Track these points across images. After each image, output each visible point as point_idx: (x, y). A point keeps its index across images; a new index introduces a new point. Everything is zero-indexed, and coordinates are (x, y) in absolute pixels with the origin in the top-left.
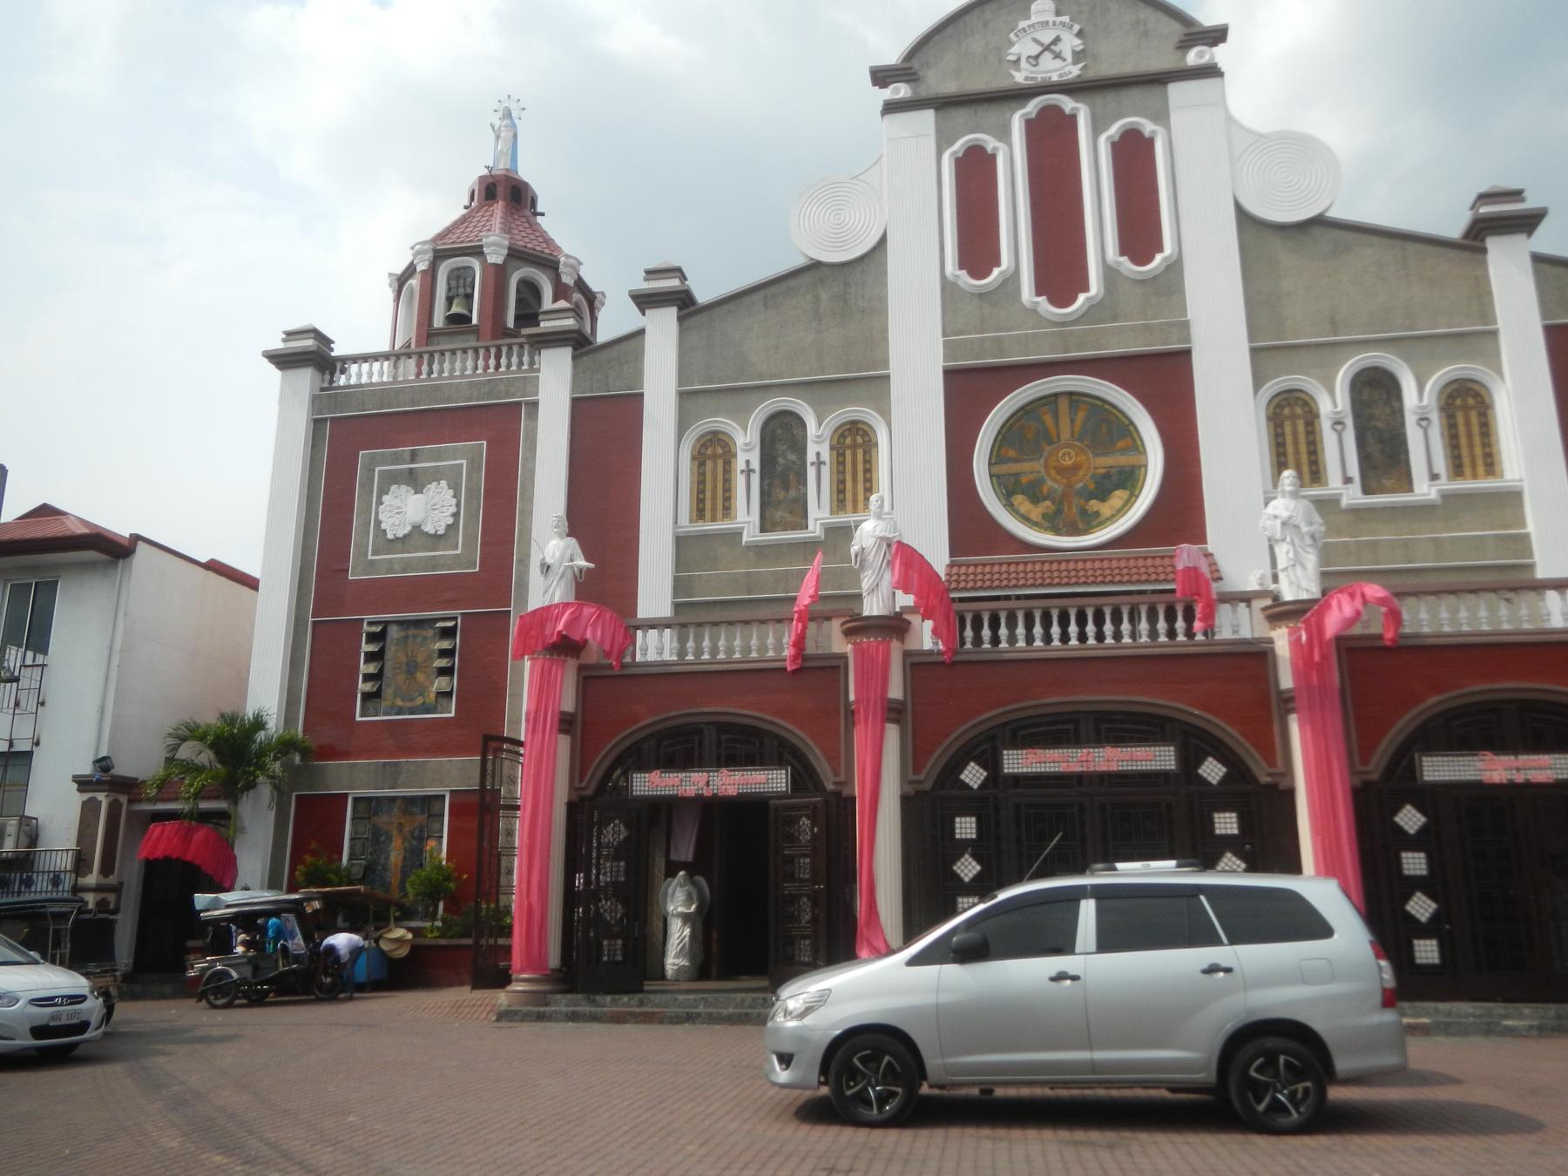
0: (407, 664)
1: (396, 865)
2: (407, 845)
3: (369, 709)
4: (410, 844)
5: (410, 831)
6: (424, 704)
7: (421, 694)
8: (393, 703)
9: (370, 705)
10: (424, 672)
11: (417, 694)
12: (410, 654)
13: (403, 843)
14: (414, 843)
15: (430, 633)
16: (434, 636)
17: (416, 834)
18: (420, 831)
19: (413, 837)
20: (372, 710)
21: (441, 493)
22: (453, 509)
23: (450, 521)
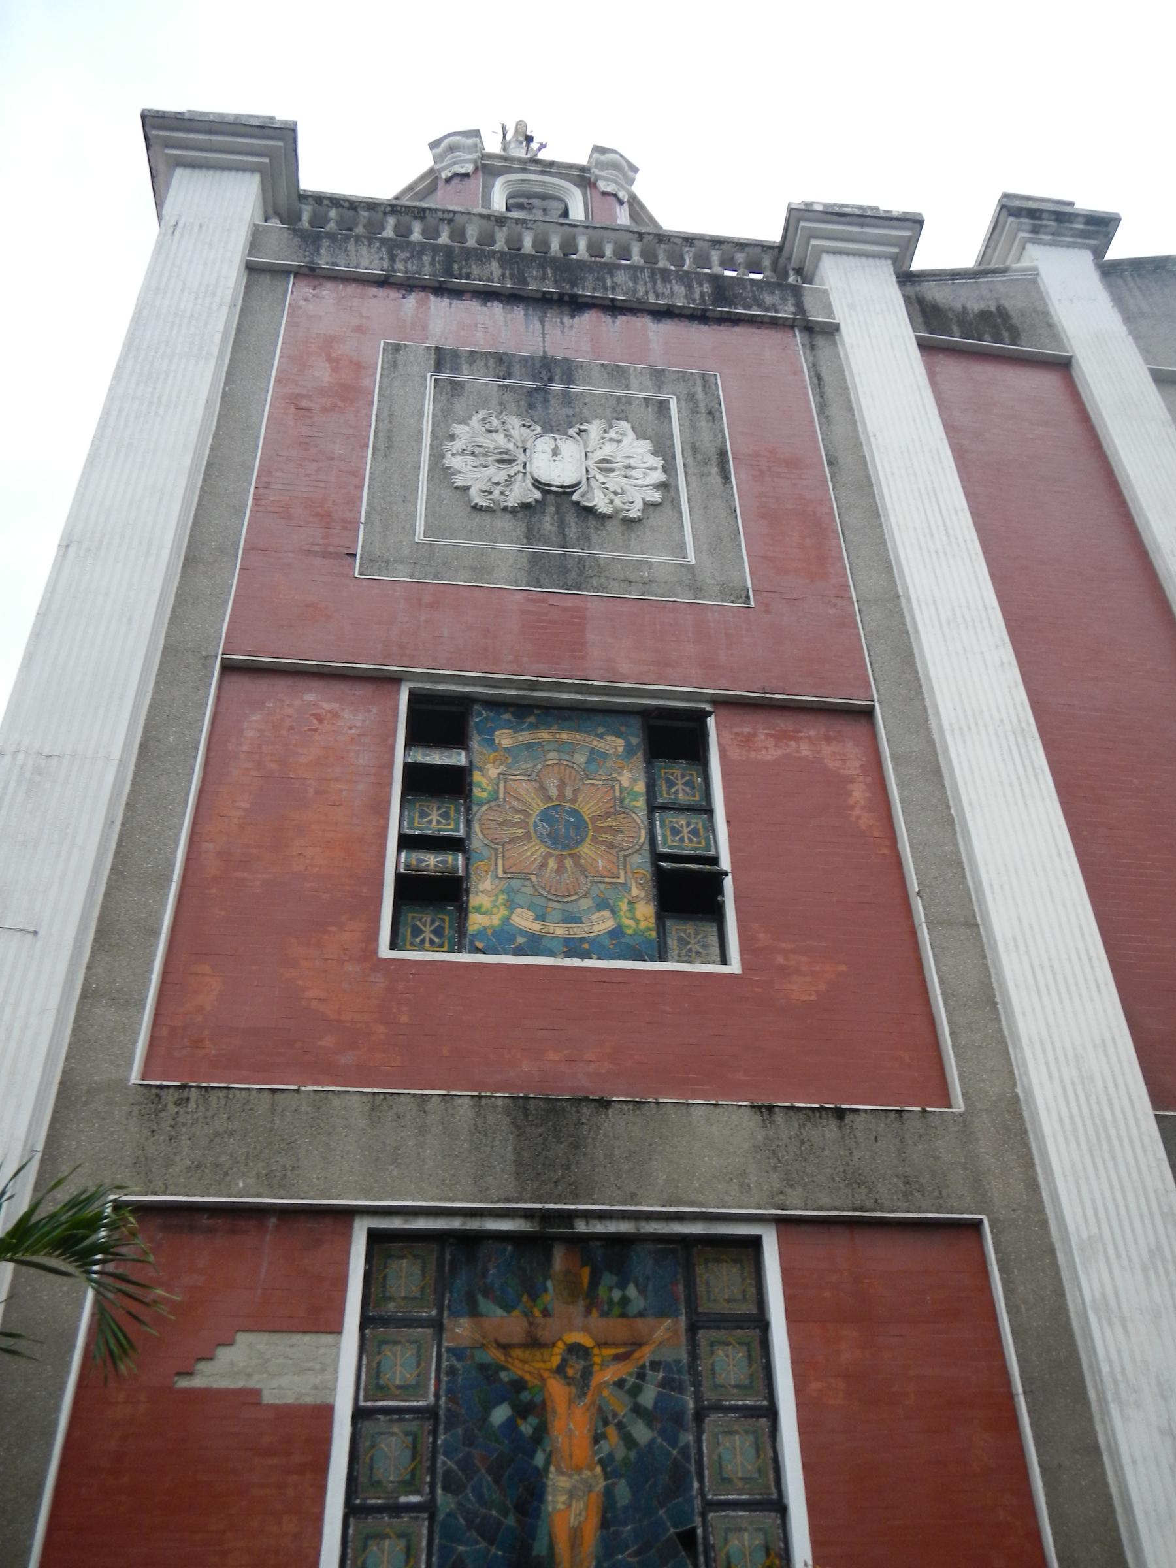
0: (545, 816)
1: (576, 1535)
2: (613, 1442)
3: (417, 932)
4: (629, 1441)
5: (620, 1384)
6: (616, 933)
7: (602, 904)
8: (507, 919)
9: (426, 922)
10: (612, 846)
11: (586, 903)
12: (554, 792)
13: (597, 1439)
14: (642, 1433)
15: (613, 744)
16: (630, 751)
17: (649, 1396)
18: (666, 1383)
19: (637, 1410)
20: (428, 935)
21: (619, 441)
22: (658, 476)
23: (656, 496)
